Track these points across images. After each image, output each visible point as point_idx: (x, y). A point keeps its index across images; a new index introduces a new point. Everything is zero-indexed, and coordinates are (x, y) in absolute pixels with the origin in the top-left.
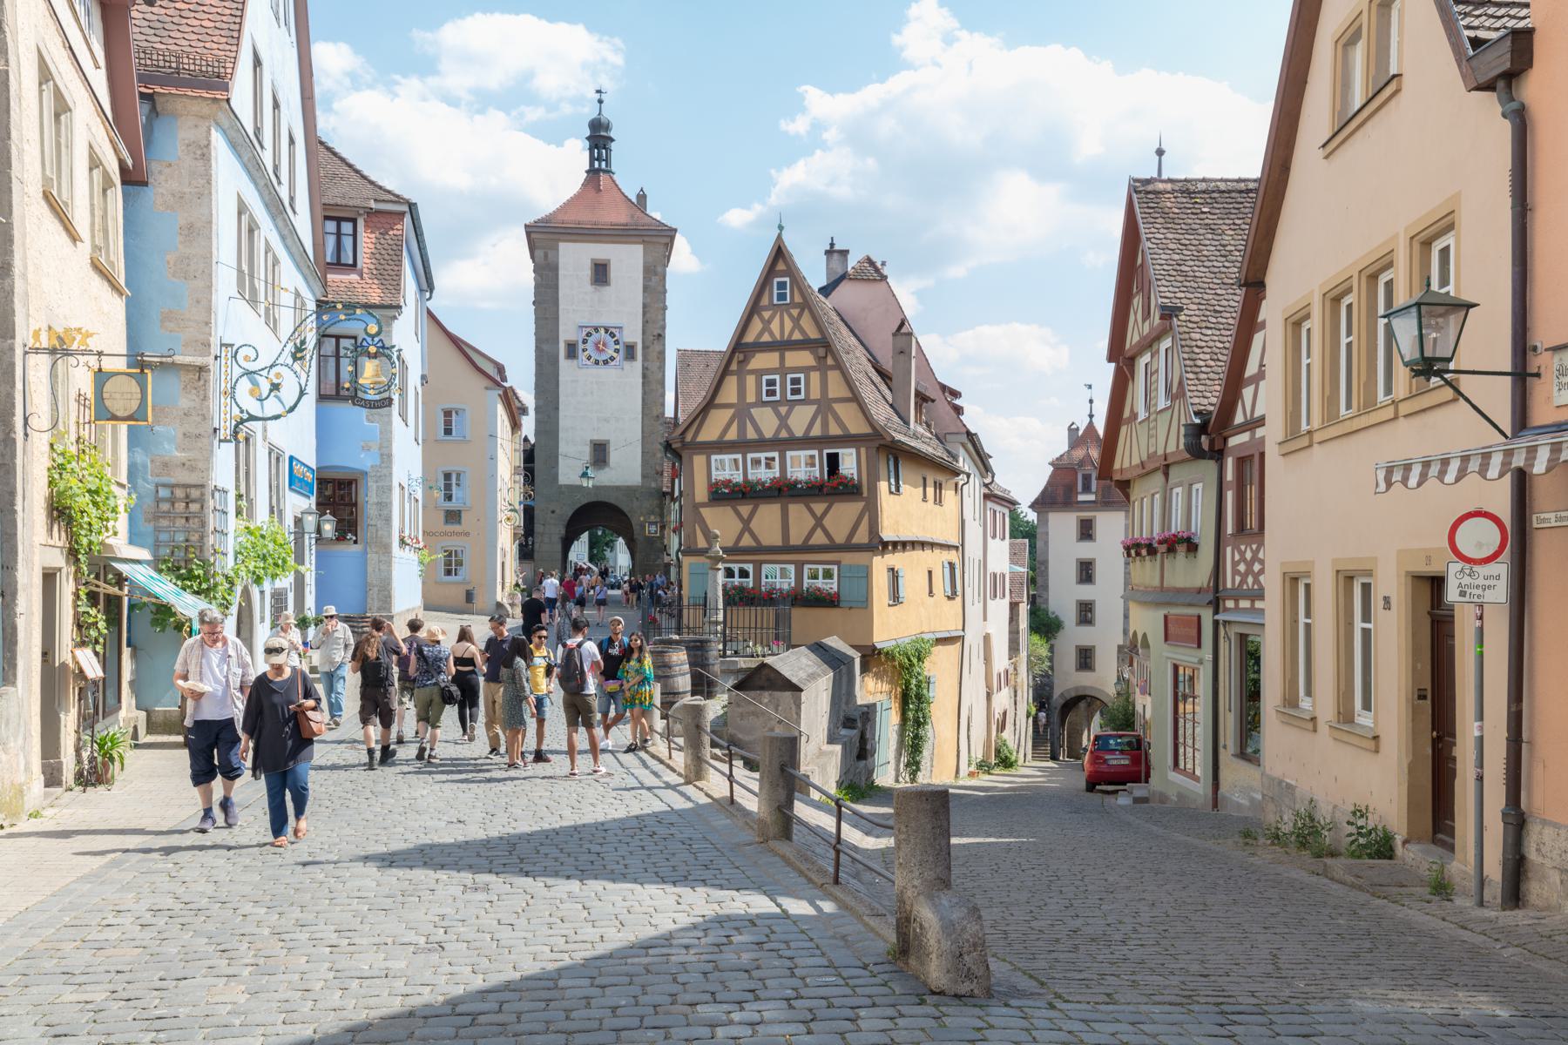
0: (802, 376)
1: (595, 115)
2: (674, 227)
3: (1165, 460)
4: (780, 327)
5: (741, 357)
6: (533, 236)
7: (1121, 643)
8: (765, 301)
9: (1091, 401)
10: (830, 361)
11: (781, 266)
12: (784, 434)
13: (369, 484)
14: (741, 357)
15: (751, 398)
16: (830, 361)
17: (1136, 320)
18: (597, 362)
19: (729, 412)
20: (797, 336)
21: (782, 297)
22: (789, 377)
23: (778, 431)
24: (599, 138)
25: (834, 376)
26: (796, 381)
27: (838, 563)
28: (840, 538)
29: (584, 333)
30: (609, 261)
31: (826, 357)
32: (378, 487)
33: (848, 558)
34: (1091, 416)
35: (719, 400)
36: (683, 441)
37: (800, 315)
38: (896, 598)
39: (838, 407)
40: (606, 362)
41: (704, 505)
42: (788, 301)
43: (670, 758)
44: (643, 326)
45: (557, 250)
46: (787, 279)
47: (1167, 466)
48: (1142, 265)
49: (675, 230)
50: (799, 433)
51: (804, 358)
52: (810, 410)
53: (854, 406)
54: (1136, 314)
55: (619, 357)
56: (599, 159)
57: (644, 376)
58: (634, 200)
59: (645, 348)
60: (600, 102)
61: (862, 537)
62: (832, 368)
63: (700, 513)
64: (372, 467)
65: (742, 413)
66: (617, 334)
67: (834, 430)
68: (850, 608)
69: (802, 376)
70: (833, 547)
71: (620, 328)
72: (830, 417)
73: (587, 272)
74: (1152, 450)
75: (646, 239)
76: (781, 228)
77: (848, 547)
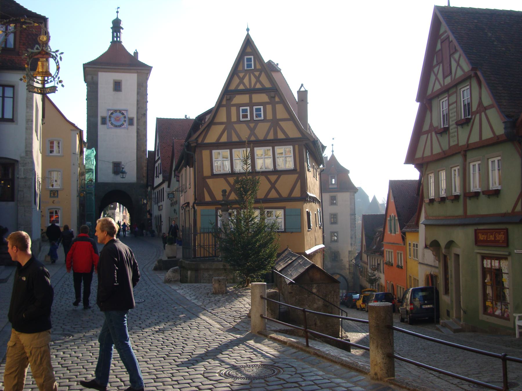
0: (262, 107)
1: (115, 18)
2: (151, 66)
3: (468, 147)
4: (248, 82)
5: (228, 97)
6: (87, 69)
7: (350, 250)
8: (240, 68)
9: (333, 145)
10: (277, 99)
11: (249, 50)
12: (253, 138)
13: (20, 168)
14: (228, 97)
15: (234, 119)
16: (277, 99)
17: (437, 79)
18: (116, 126)
19: (223, 127)
20: (258, 86)
21: (249, 66)
22: (255, 108)
23: (250, 136)
24: (117, 26)
25: (280, 108)
26: (258, 110)
27: (284, 208)
28: (285, 194)
29: (110, 113)
30: (122, 80)
31: (274, 97)
32: (24, 169)
33: (289, 205)
34: (333, 151)
35: (217, 120)
36: (197, 143)
37: (260, 75)
38: (309, 227)
39: (282, 123)
40: (120, 126)
41: (209, 177)
42: (253, 68)
43: (307, 345)
44: (137, 110)
45: (97, 75)
46: (252, 57)
47: (466, 151)
48: (440, 50)
49: (152, 67)
50: (261, 137)
51: (263, 98)
52: (267, 125)
53: (291, 123)
54: (436, 76)
55: (126, 124)
56: (117, 37)
57: (138, 132)
58: (133, 54)
59: (138, 119)
60: (117, 12)
61: (297, 193)
62: (278, 103)
63: (206, 182)
64: (21, 157)
65: (229, 125)
66: (125, 113)
67: (281, 136)
68: (292, 232)
69: (262, 107)
70: (281, 199)
71: (127, 111)
72: (278, 128)
73: (111, 86)
74: (452, 144)
75: (139, 71)
76: (248, 30)
77: (290, 199)
